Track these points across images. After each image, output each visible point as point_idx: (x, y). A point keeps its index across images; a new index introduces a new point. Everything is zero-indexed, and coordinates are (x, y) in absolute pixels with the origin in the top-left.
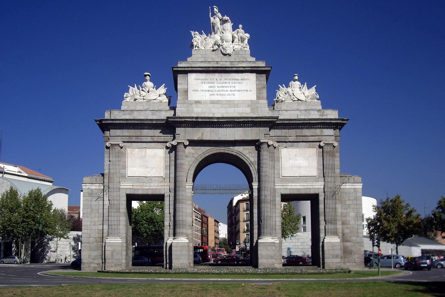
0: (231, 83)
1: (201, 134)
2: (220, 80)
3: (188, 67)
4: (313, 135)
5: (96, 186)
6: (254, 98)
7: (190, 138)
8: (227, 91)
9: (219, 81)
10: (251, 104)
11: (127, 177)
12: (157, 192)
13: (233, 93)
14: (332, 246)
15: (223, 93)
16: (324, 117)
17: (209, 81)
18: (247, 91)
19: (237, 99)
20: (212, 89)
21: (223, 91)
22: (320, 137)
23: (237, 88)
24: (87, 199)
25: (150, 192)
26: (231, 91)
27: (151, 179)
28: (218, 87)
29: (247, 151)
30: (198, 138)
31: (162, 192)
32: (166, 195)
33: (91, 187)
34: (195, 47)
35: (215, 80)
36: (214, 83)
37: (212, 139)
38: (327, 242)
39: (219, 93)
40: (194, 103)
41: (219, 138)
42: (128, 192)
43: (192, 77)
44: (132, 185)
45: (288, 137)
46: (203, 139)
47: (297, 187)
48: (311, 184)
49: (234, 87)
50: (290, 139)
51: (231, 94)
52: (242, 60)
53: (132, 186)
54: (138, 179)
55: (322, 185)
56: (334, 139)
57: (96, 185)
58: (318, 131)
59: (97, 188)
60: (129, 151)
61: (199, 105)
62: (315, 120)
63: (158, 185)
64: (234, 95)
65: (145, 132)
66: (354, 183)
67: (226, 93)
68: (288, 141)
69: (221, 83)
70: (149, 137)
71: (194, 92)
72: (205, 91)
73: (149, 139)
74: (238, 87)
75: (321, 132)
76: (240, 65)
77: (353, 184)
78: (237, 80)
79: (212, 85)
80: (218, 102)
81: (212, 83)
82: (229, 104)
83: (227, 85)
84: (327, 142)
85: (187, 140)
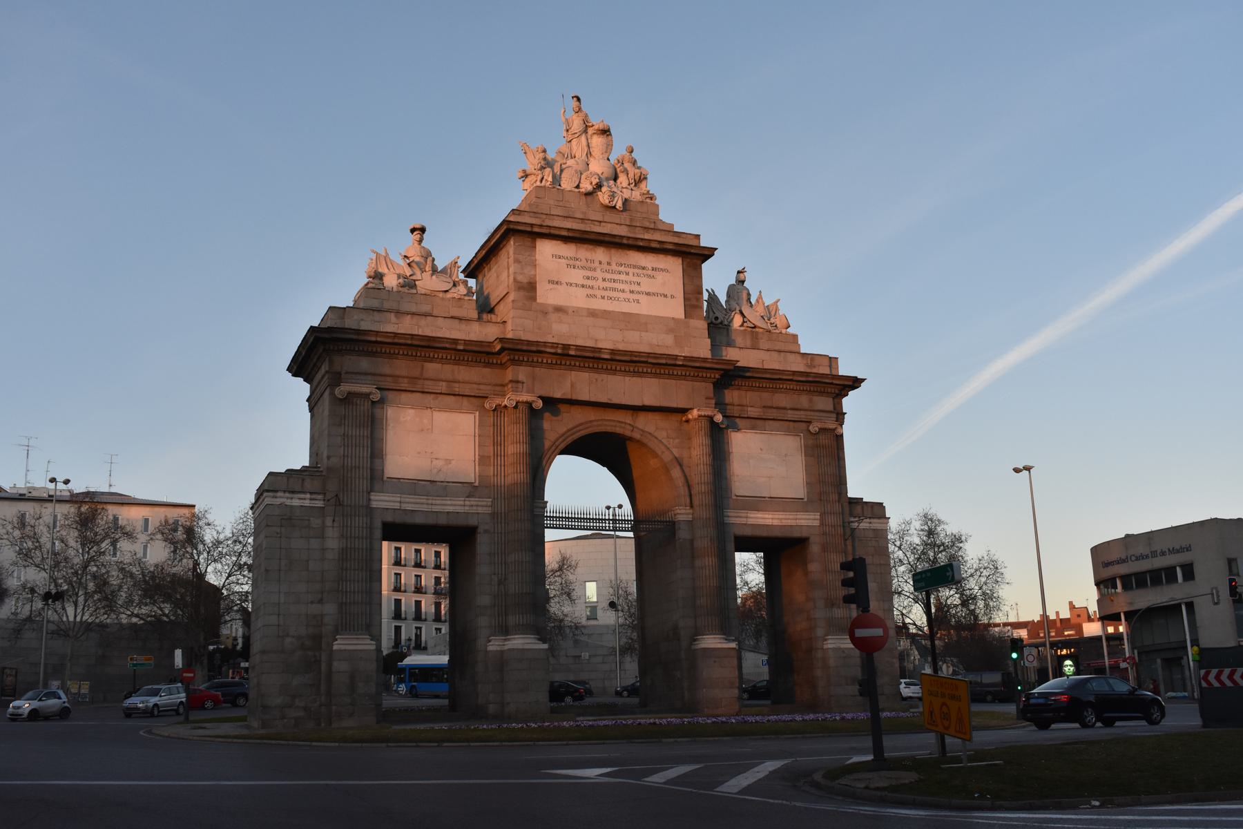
0: (631, 274)
2: (609, 264)
3: (541, 226)
4: (796, 407)
5: (302, 499)
6: (679, 313)
8: (623, 291)
9: (605, 266)
10: (671, 326)
11: (385, 479)
12: (461, 522)
13: (635, 296)
16: (815, 370)
17: (584, 263)
18: (665, 296)
19: (644, 312)
20: (590, 283)
21: (614, 290)
22: (809, 413)
23: (644, 288)
24: (278, 533)
25: (443, 521)
26: (632, 292)
28: (604, 280)
29: (664, 434)
30: (564, 394)
31: (472, 522)
32: (481, 529)
33: (288, 502)
34: (541, 181)
35: (597, 264)
36: (595, 270)
37: (593, 399)
38: (833, 649)
40: (550, 309)
41: (609, 399)
42: (389, 519)
43: (546, 250)
44: (399, 499)
45: (746, 408)
46: (574, 397)
47: (768, 521)
48: (795, 517)
50: (752, 413)
51: (631, 300)
52: (647, 224)
53: (398, 504)
54: (414, 486)
56: (835, 419)
57: (302, 496)
58: (804, 400)
59: (307, 503)
60: (390, 412)
61: (560, 314)
63: (462, 503)
65: (432, 368)
66: (873, 518)
67: (621, 295)
68: (746, 416)
69: (610, 271)
70: (441, 383)
71: (551, 286)
72: (577, 285)
73: (443, 387)
74: (646, 285)
75: (811, 401)
76: (647, 236)
77: (872, 520)
78: (644, 268)
79: (589, 274)
80: (606, 314)
81: (590, 269)
82: (629, 322)
83: (623, 277)
85: (539, 397)
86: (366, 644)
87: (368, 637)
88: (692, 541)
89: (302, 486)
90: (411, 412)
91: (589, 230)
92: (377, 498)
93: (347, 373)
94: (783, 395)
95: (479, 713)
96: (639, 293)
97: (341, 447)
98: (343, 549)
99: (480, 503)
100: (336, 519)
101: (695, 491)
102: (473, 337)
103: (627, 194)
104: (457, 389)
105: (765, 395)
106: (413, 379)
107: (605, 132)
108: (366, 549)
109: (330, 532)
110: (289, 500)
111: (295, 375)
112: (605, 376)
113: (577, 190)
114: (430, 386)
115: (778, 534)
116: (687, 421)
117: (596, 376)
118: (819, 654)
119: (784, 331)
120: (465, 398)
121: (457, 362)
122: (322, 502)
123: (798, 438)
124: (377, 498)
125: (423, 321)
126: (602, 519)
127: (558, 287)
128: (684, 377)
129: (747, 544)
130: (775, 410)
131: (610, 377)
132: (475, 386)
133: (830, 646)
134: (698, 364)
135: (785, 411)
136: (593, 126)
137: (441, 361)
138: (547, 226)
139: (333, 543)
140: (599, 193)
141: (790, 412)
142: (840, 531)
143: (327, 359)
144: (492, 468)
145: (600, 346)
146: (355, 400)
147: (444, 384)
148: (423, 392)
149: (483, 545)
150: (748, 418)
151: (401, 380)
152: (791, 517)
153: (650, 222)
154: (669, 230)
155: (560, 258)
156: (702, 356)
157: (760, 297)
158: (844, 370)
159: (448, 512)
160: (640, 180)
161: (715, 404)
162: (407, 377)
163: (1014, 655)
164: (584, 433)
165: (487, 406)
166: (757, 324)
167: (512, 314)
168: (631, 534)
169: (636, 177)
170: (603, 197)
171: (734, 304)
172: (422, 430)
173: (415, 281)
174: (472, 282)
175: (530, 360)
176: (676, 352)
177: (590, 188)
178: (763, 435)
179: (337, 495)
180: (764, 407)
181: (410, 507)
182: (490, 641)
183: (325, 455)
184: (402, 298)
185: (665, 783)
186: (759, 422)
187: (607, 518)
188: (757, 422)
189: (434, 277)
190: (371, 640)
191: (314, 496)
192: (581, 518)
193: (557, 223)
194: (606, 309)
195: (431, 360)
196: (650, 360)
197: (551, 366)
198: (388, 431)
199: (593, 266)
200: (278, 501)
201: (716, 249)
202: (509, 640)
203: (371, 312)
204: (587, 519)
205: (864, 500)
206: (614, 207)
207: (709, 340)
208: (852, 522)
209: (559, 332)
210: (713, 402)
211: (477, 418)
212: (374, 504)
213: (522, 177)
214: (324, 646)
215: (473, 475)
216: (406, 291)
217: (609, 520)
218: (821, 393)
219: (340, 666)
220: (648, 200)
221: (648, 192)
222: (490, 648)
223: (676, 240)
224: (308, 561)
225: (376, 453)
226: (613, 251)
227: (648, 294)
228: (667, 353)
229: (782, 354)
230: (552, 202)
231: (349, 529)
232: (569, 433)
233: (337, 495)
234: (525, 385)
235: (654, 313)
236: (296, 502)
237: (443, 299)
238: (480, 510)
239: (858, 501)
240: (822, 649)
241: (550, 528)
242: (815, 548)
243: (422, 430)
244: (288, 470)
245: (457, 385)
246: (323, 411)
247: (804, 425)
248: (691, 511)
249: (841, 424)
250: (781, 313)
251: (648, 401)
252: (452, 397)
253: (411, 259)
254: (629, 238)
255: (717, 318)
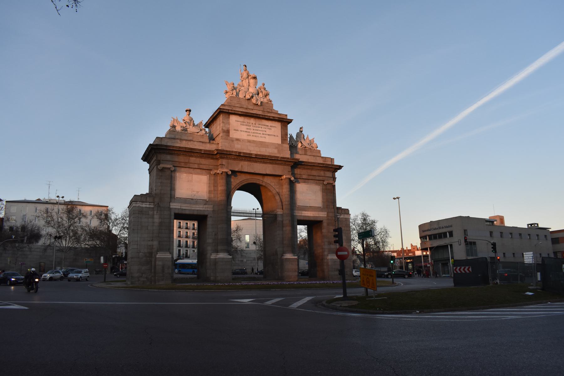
1: (240, 166)
2: (255, 124)
3: (232, 110)
5: (146, 204)
6: (280, 142)
7: (232, 169)
8: (260, 134)
9: (254, 125)
10: (277, 146)
11: (175, 198)
12: (202, 213)
14: (334, 262)
15: (257, 135)
16: (326, 163)
17: (246, 124)
18: (275, 136)
21: (257, 133)
24: (137, 216)
25: (196, 213)
26: (263, 134)
27: (197, 201)
28: (253, 130)
30: (239, 169)
31: (206, 213)
32: (209, 216)
33: (141, 206)
34: (232, 95)
35: (251, 124)
36: (250, 126)
37: (249, 171)
39: (254, 134)
41: (255, 171)
42: (177, 212)
43: (233, 118)
44: (180, 205)
46: (242, 171)
47: (309, 214)
48: (318, 213)
49: (266, 131)
52: (269, 110)
53: (180, 207)
55: (325, 214)
57: (146, 203)
58: (322, 173)
59: (148, 206)
60: (178, 174)
61: (238, 141)
62: (322, 165)
63: (202, 207)
64: (265, 137)
65: (192, 159)
66: (345, 214)
67: (259, 135)
70: (195, 165)
72: (244, 131)
73: (196, 166)
74: (268, 132)
75: (324, 173)
76: (269, 115)
77: (345, 215)
79: (248, 127)
80: (254, 142)
81: (249, 126)
83: (260, 129)
84: (329, 182)
85: (230, 170)
86: (168, 256)
87: (169, 253)
88: (282, 221)
89: (146, 200)
90: (185, 174)
91: (248, 112)
92: (173, 204)
93: (162, 160)
94: (315, 171)
95: (207, 280)
96: (265, 134)
97: (160, 186)
98: (160, 222)
99: (209, 207)
100: (158, 212)
101: (284, 204)
102: (207, 149)
103: (262, 100)
104: (201, 167)
105: (309, 171)
106: (186, 163)
107: (255, 78)
108: (169, 222)
109: (156, 216)
110: (141, 205)
111: (144, 161)
112: (253, 163)
113: (244, 98)
114: (192, 166)
115: (312, 219)
116: (282, 180)
117: (250, 163)
118: (326, 261)
119: (316, 149)
120: (204, 170)
121: (201, 157)
122: (153, 206)
123: (320, 186)
124: (173, 204)
125: (190, 143)
126: (251, 213)
127: (236, 131)
128: (281, 164)
129: (301, 222)
130: (312, 176)
131: (255, 164)
132: (208, 166)
133: (329, 258)
134: (286, 160)
135: (315, 177)
136: (250, 76)
137: (196, 157)
138: (234, 110)
139: (157, 220)
140: (252, 99)
141: (317, 177)
142: (334, 218)
143: (155, 156)
144: (213, 195)
145: (252, 152)
146: (165, 170)
147: (197, 165)
148: (189, 168)
149: (210, 221)
150: (303, 179)
151: (181, 163)
152: (317, 213)
153: (270, 110)
154: (276, 113)
155: (238, 122)
156: (287, 157)
157: (308, 137)
158: (336, 163)
159: (197, 210)
160: (267, 95)
161: (292, 174)
162: (184, 162)
163: (392, 262)
164: (245, 183)
165: (212, 173)
166: (307, 146)
167: (221, 141)
168: (261, 219)
169: (266, 94)
170: (254, 101)
171: (298, 139)
172: (189, 181)
173: (187, 128)
174: (207, 130)
175: (227, 157)
176: (278, 155)
177: (249, 97)
178: (307, 185)
179: (158, 203)
180: (308, 175)
181: (184, 208)
182: (212, 255)
183: (154, 189)
184: (182, 134)
185: (271, 304)
186: (307, 180)
187: (253, 213)
188: (306, 180)
189: (194, 127)
190: (170, 254)
191: (150, 204)
192: (244, 213)
193: (237, 109)
194: (254, 140)
195: (192, 156)
196: (269, 158)
197: (234, 159)
198: (177, 181)
199: (250, 125)
200: (138, 205)
201: (293, 120)
202: (218, 254)
203: (171, 139)
204: (246, 213)
205: (342, 208)
206: (258, 104)
207: (290, 152)
208: (338, 215)
209: (238, 147)
210: (291, 173)
211: (208, 177)
212: (171, 207)
213: (225, 93)
214: (153, 256)
215: (206, 197)
216: (184, 132)
217: (254, 213)
218: (328, 171)
219: (159, 263)
220: (269, 102)
221: (270, 99)
222: (212, 257)
223: (279, 116)
224: (148, 226)
225: (172, 189)
226: (257, 120)
227: (269, 135)
228: (275, 156)
229: (315, 157)
230: (235, 102)
231: (162, 215)
232: (240, 183)
233: (158, 203)
234: (225, 166)
235: (270, 142)
236: (144, 206)
237: (197, 135)
238: (209, 209)
239: (340, 208)
240: (327, 259)
241: (233, 216)
242: (325, 224)
243: (189, 181)
244: (141, 194)
245: (201, 165)
246: (154, 174)
247: (322, 182)
248: (282, 211)
249: (335, 182)
250: (315, 142)
251: (268, 172)
252: (199, 170)
253: (186, 121)
254: (262, 115)
255: (292, 144)
